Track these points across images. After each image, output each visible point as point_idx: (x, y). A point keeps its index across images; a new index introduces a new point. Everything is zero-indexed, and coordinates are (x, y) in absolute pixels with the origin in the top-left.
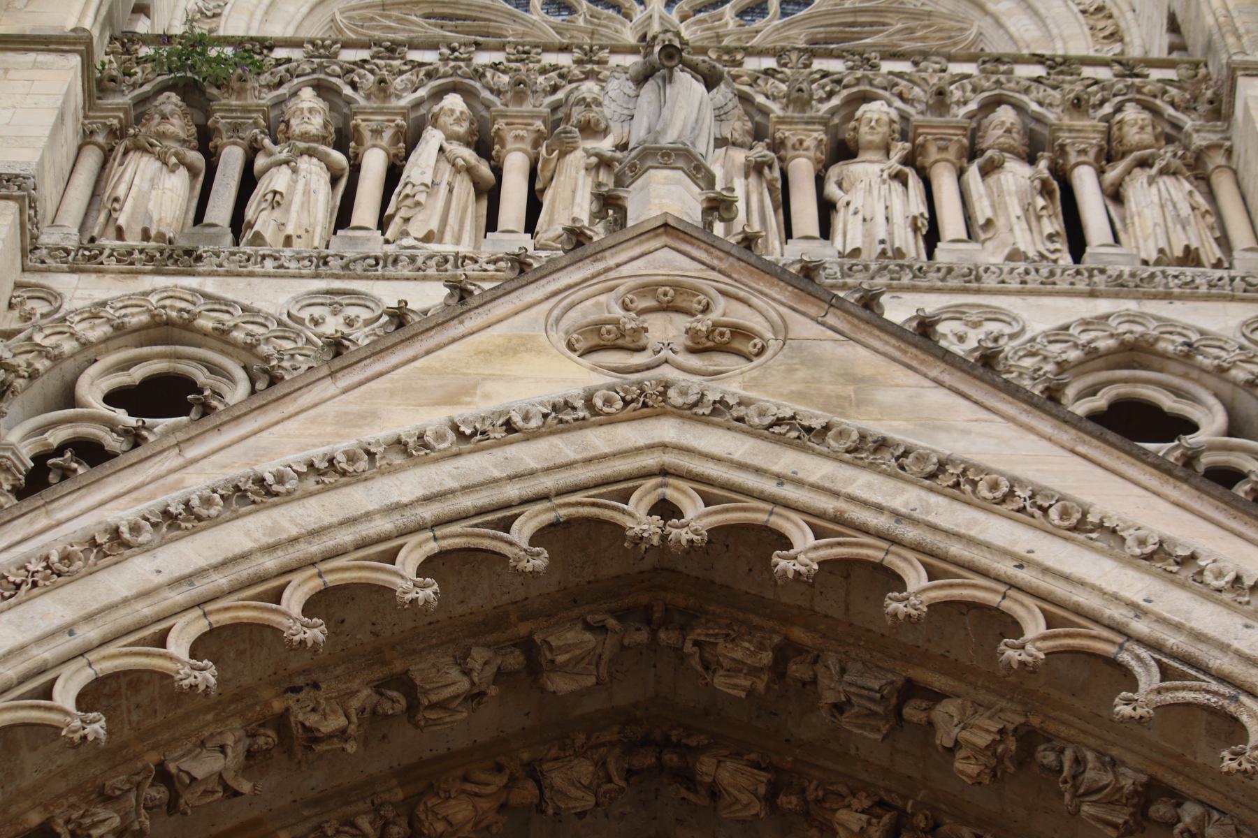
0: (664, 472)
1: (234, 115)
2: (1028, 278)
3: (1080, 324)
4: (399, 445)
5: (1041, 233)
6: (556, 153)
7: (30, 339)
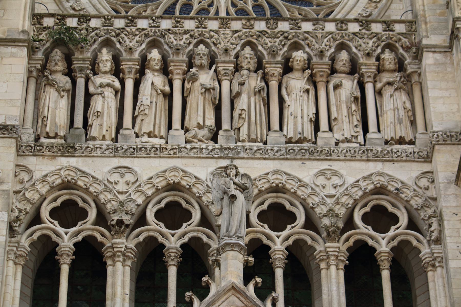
1: (80, 62)
2: (347, 154)
3: (363, 179)
5: (353, 123)
6: (191, 82)
7: (24, 194)
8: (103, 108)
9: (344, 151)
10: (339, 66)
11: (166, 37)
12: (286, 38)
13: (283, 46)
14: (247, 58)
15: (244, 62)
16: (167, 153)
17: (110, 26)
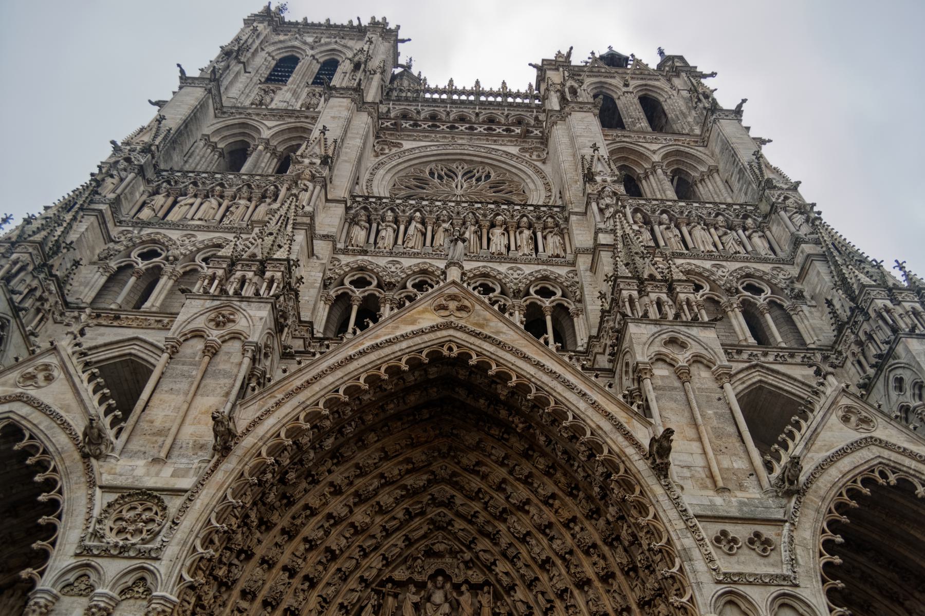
0: (450, 341)
4: (402, 336)
10: (522, 224)
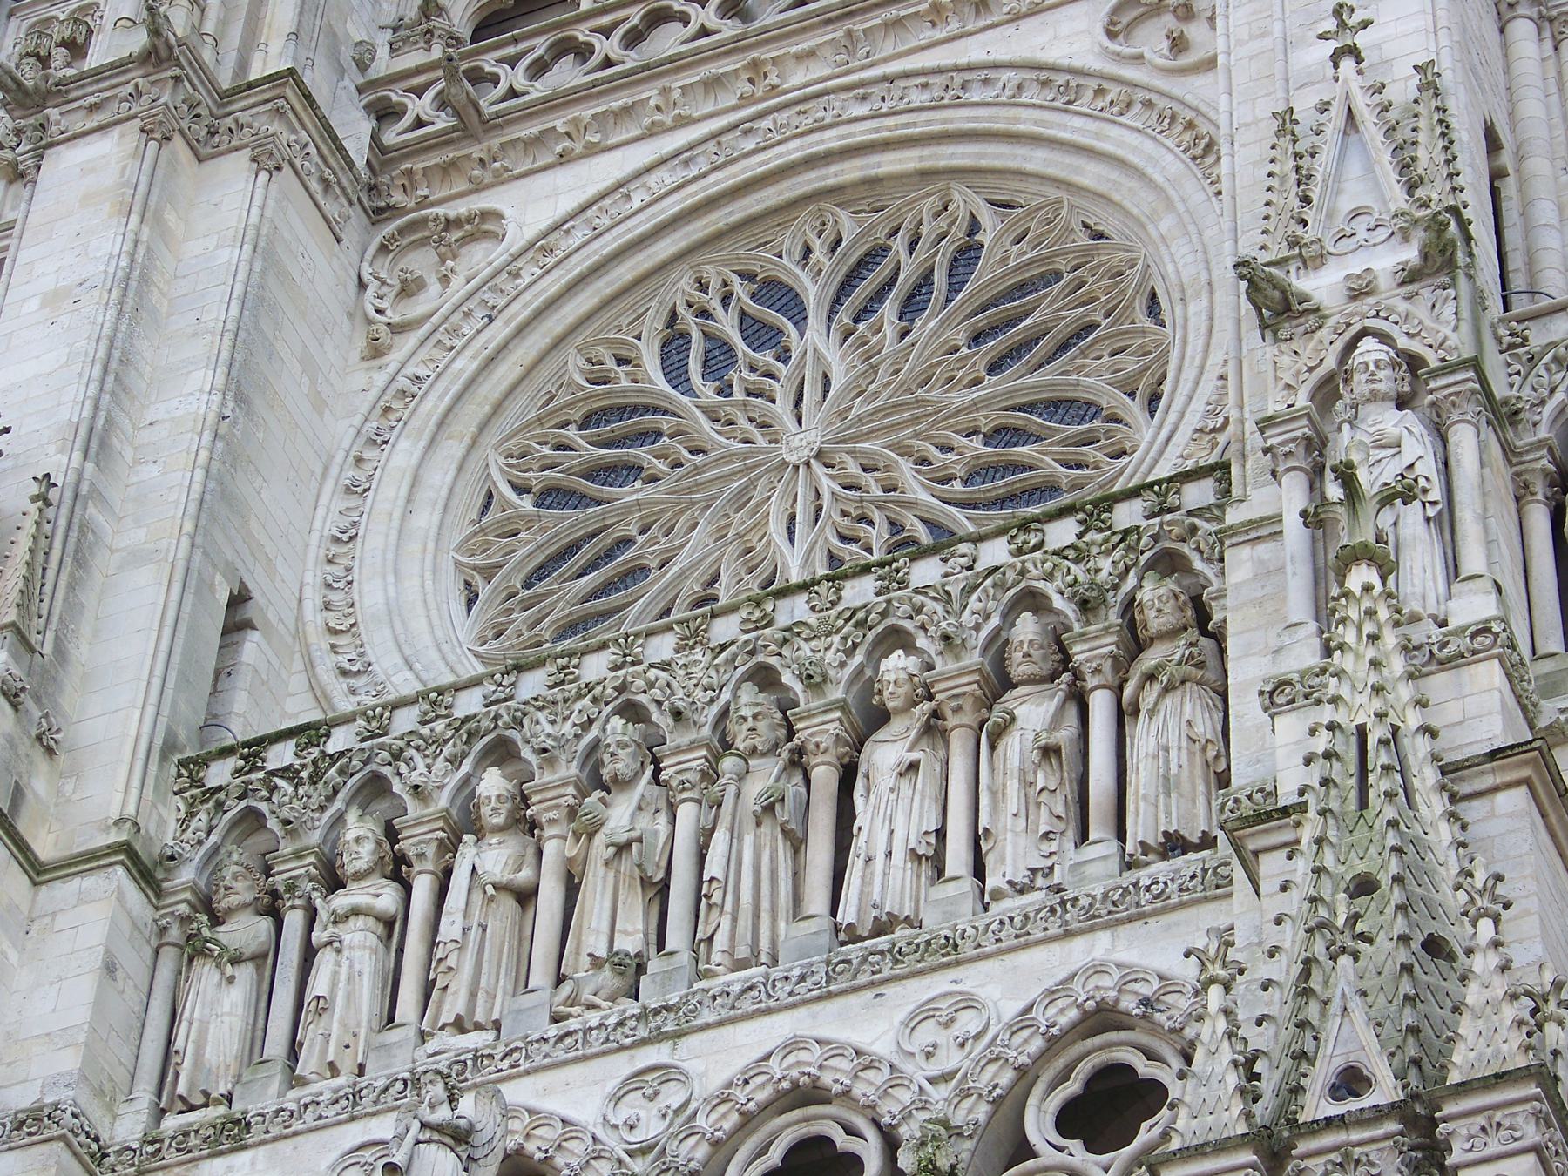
2: (1002, 935)
8: (334, 985)
9: (994, 926)
11: (526, 722)
12: (860, 624)
13: (850, 652)
14: (745, 719)
15: (740, 731)
16: (492, 1068)
17: (381, 736)
